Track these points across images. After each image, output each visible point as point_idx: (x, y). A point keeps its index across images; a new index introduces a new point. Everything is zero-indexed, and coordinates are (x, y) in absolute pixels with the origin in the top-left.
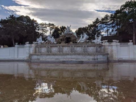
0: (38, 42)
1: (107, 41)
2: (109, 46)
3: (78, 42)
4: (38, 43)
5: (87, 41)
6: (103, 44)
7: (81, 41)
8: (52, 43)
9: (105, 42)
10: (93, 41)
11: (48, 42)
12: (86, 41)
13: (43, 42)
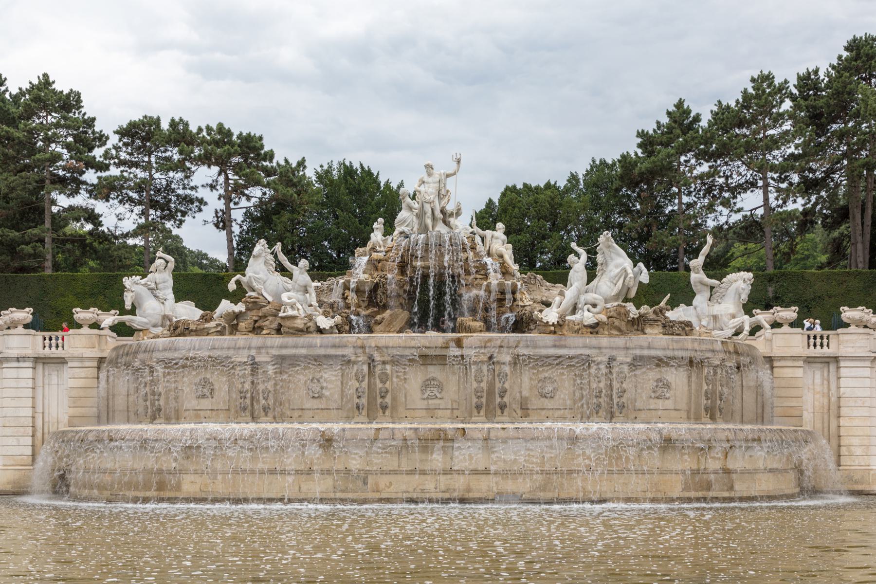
0: (133, 312)
1: (790, 313)
2: (809, 361)
3: (551, 316)
4: (136, 321)
5: (633, 311)
6: (761, 345)
7: (574, 310)
8: (299, 324)
9: (776, 325)
10: (672, 315)
11: (254, 315)
12: (622, 314)
13: (188, 311)
